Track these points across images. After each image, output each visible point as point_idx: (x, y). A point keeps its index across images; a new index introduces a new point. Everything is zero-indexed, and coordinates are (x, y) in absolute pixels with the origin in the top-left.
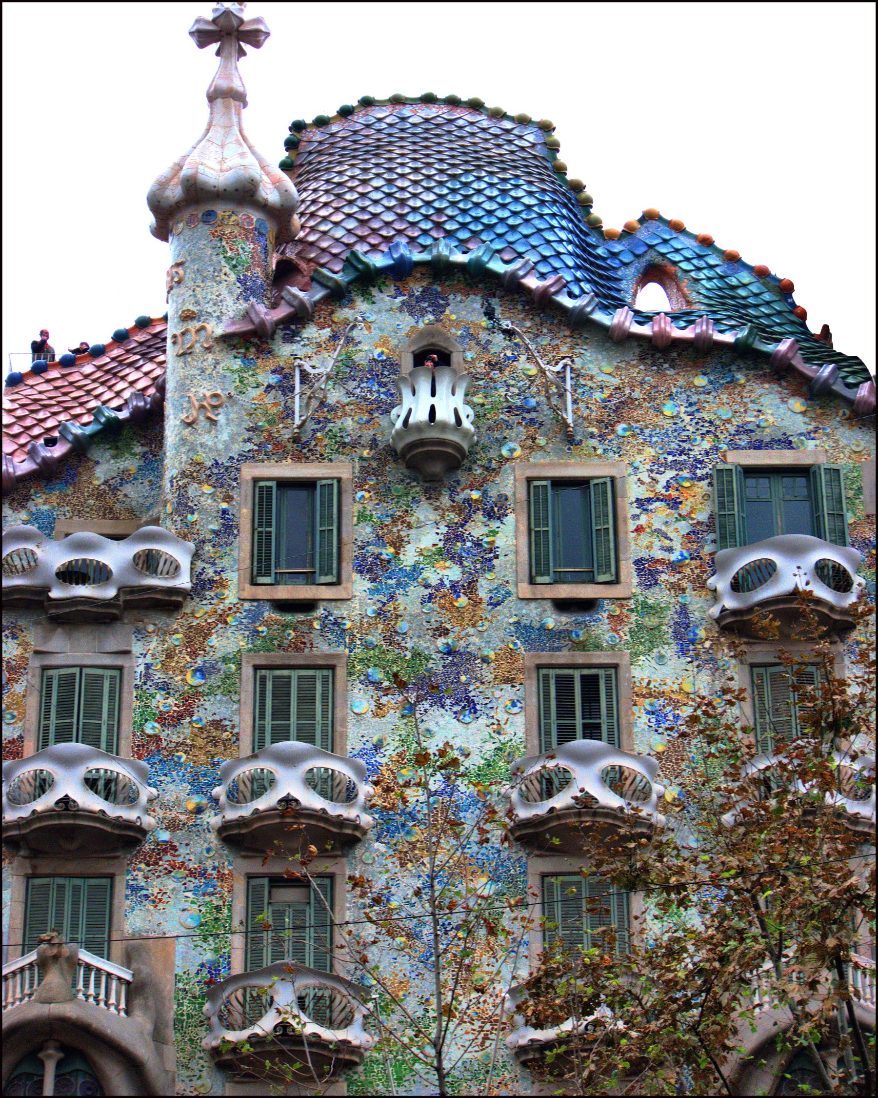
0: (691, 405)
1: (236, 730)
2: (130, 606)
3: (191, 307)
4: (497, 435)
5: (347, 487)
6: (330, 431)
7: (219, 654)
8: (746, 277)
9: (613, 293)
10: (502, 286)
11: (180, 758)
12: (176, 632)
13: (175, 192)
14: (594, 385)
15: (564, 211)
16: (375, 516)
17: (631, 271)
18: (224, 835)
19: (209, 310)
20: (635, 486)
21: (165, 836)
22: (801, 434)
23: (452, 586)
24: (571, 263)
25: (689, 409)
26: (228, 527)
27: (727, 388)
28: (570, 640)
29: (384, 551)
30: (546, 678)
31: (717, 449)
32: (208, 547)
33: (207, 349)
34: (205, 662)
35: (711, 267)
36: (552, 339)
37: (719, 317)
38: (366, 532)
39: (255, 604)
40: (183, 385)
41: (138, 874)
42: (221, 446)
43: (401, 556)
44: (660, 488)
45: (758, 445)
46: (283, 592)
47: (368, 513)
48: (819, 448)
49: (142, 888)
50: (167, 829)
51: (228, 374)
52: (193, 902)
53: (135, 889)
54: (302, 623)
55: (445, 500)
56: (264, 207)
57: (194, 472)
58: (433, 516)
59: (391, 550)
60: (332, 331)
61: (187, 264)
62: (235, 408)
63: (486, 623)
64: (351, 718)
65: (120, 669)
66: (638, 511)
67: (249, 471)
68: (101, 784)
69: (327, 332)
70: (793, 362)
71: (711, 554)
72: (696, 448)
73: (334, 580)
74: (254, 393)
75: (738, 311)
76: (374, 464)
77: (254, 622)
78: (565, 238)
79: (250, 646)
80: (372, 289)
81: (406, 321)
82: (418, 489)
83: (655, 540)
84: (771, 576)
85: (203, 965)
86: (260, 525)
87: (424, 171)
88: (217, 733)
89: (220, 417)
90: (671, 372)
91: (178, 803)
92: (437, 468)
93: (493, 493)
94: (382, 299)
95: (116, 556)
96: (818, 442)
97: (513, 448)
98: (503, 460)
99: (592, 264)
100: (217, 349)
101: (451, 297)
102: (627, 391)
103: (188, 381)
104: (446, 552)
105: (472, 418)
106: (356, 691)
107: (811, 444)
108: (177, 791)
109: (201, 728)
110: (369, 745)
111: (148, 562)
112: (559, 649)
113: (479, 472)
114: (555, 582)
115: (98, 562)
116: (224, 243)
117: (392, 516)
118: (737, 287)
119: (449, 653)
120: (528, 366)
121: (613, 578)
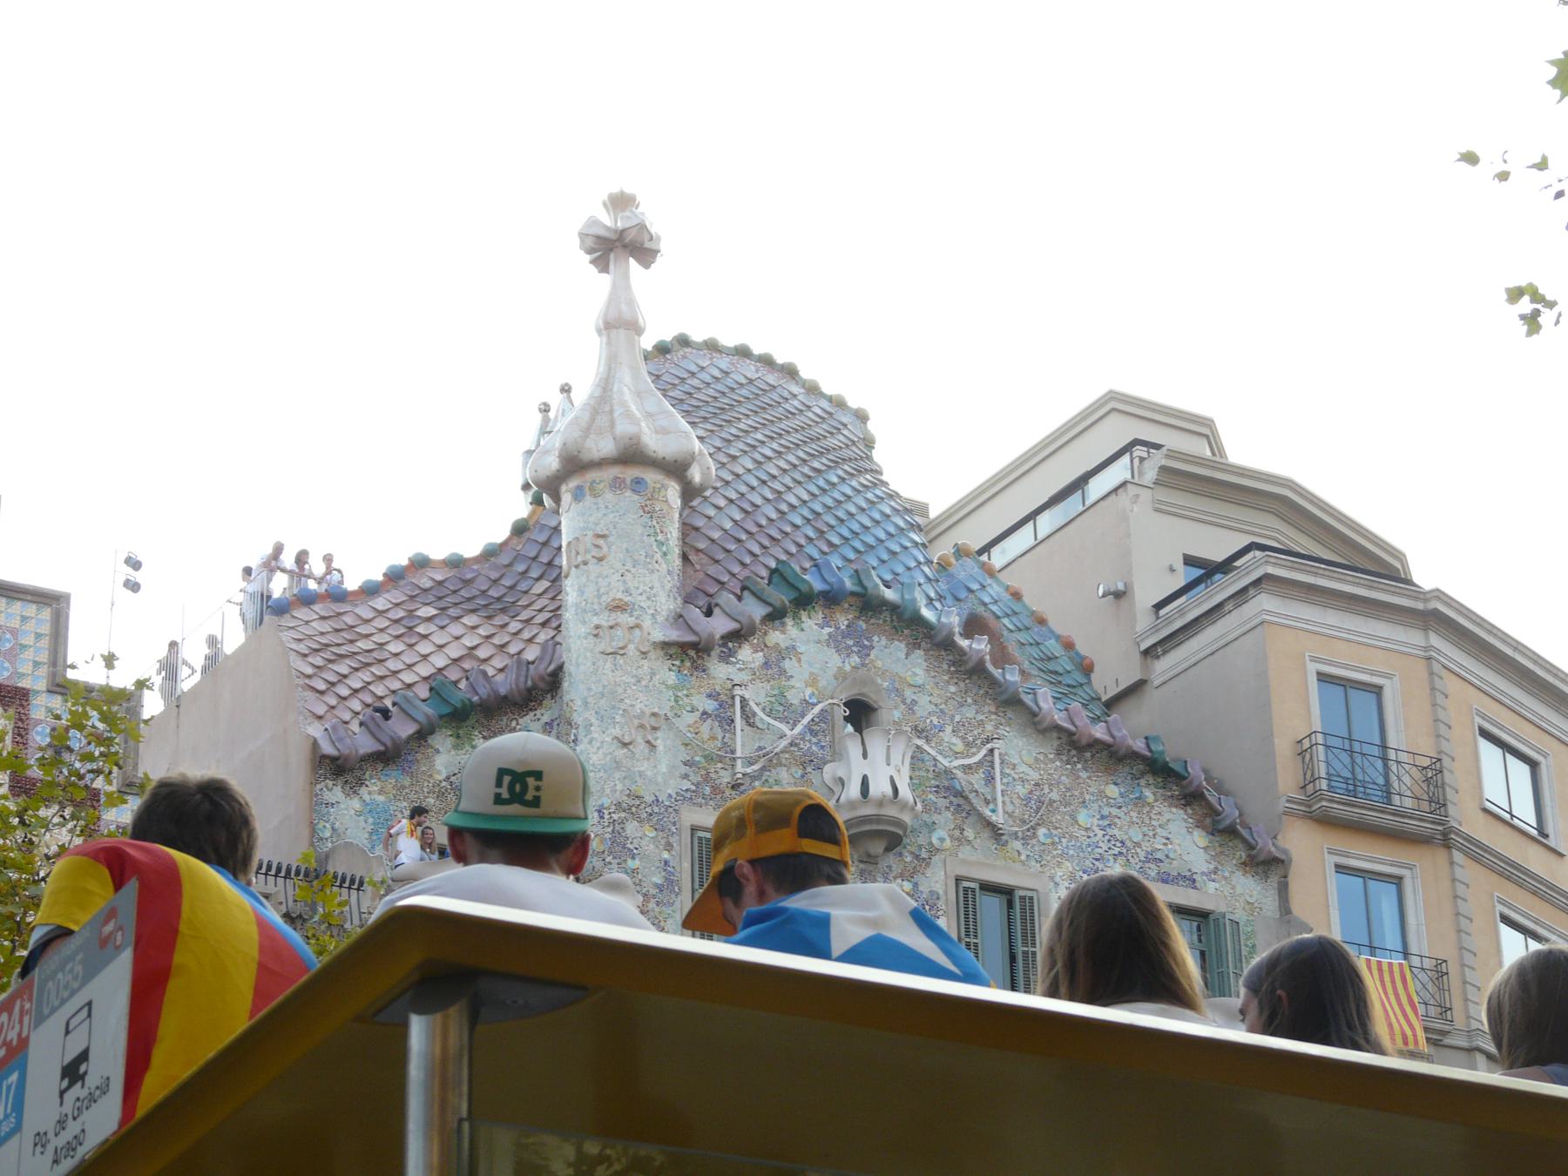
0: (1103, 817)
22: (1203, 873)
27: (1136, 805)
61: (611, 539)
90: (1084, 775)
92: (877, 847)
100: (652, 655)
101: (876, 638)
107: (1212, 885)
120: (954, 740)
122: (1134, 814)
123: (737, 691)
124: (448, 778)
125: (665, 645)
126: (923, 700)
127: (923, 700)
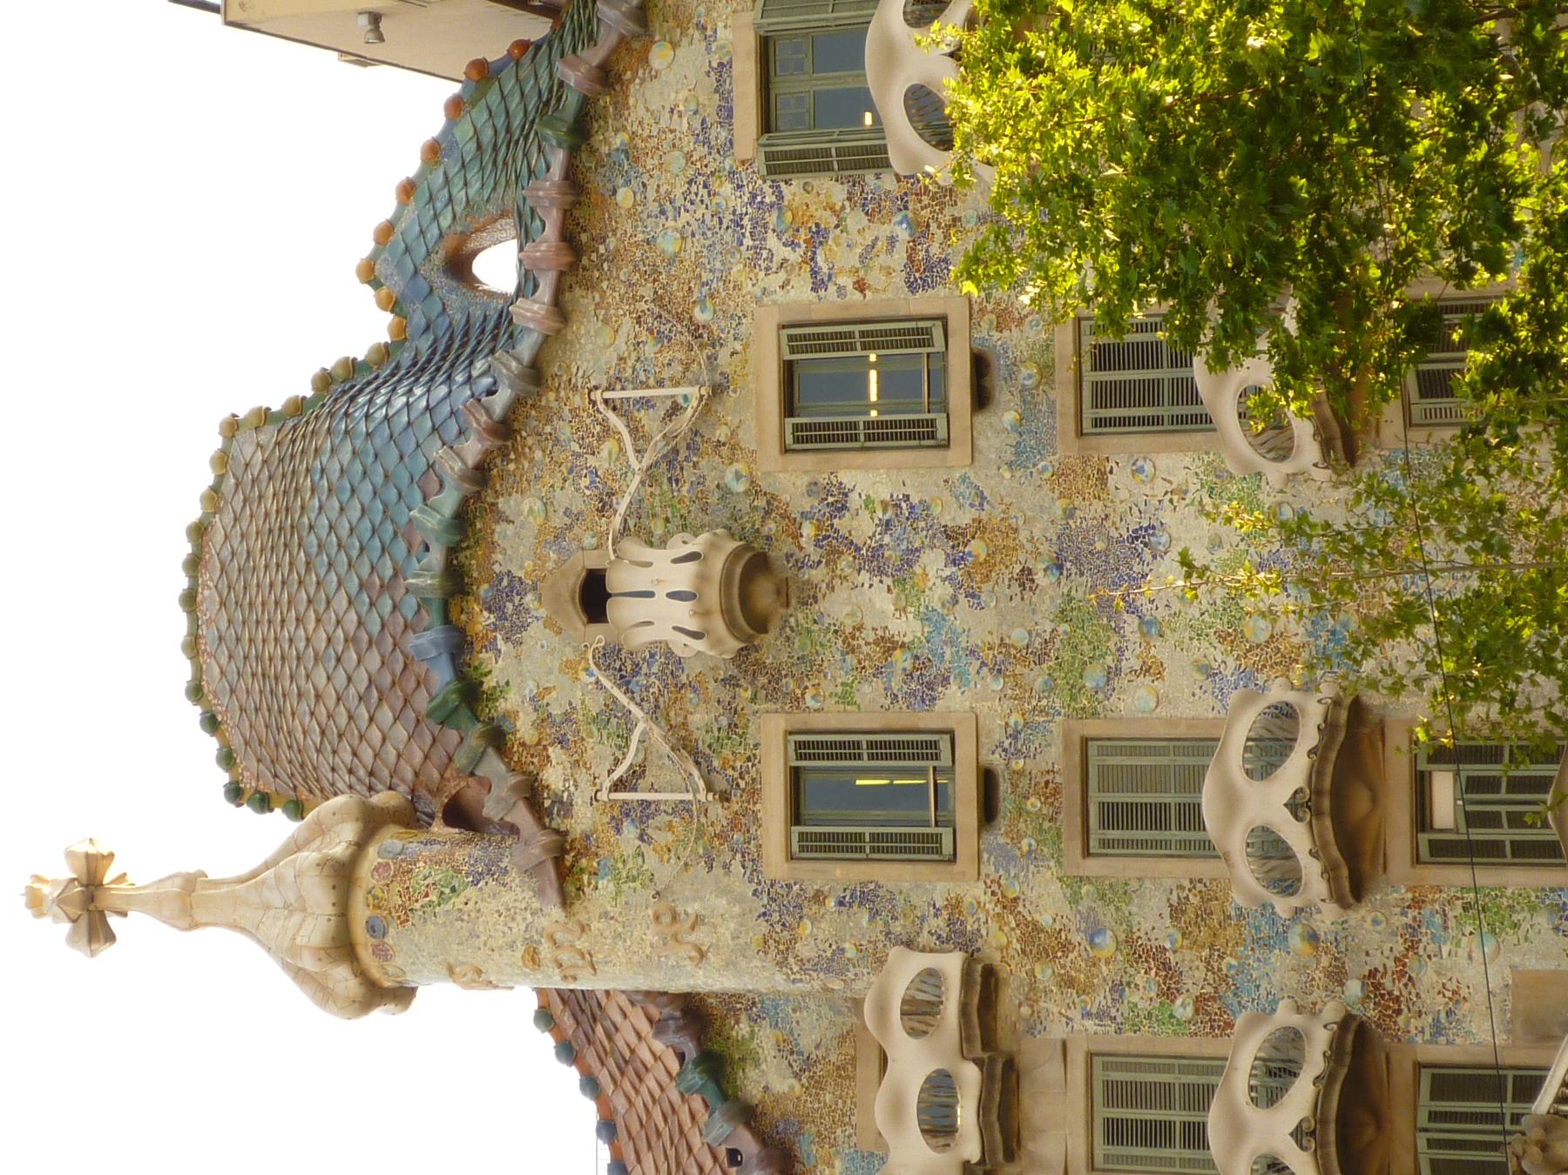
0: (663, 212)
1: (1187, 884)
2: (988, 1042)
3: (519, 954)
4: (713, 499)
5: (799, 720)
6: (710, 746)
7: (1066, 909)
8: (464, 131)
9: (489, 327)
10: (479, 493)
11: (1230, 967)
12: (1031, 973)
13: (342, 977)
14: (634, 356)
15: (361, 400)
16: (844, 679)
17: (454, 300)
18: (1351, 900)
19: (523, 927)
20: (792, 293)
21: (1354, 988)
22: (708, 49)
23: (954, 563)
24: (444, 390)
25: (670, 214)
26: (864, 897)
28: (1037, 387)
29: (900, 665)
30: (1098, 422)
31: (732, 173)
32: (897, 928)
33: (583, 930)
34: (1078, 930)
35: (447, 181)
36: (561, 418)
37: (525, 170)
38: (870, 692)
39: (985, 856)
40: (639, 964)
41: (1413, 1026)
42: (737, 909)
43: (906, 640)
44: (794, 256)
45: (727, 114)
46: (966, 811)
47: (839, 689)
48: (729, 22)
49: (1437, 1021)
50: (1342, 984)
51: (622, 899)
52: (1458, 945)
53: (1437, 1029)
54: (1014, 785)
55: (818, 575)
56: (361, 845)
57: (780, 948)
58: (842, 592)
59: (898, 653)
60: (552, 744)
61: (452, 961)
62: (676, 887)
63: (1012, 513)
64: (1163, 712)
65: (1091, 1056)
66: (832, 289)
67: (775, 863)
68: (1273, 1083)
69: (554, 752)
70: (595, 62)
71: (899, 180)
72: (731, 204)
73: (947, 737)
74: (652, 861)
75: (517, 142)
76: (763, 680)
77: (1014, 857)
78: (404, 399)
79: (1052, 863)
80: (485, 687)
81: (536, 633)
82: (800, 616)
83: (876, 263)
84: (930, 93)
85: (1556, 929)
86: (862, 850)
87: (302, 609)
88: (1198, 913)
89: (689, 910)
90: (612, 242)
91: (1301, 968)
93: (807, 504)
94: (501, 670)
95: (913, 1062)
96: (720, 25)
97: (733, 477)
98: (755, 490)
99: (444, 359)
102: (642, 306)
103: (629, 959)
104: (901, 574)
105: (686, 536)
106: (1122, 705)
107: (722, 34)
108: (1279, 970)
109: (1184, 935)
110: (1208, 684)
111: (920, 1013)
112: (1052, 405)
113: (773, 526)
114: (944, 408)
115: (922, 1090)
116: (417, 906)
117: (844, 654)
118: (479, 147)
119: (1060, 567)
120: (604, 454)
121: (939, 323)
122: (650, 163)
123: (603, 796)
124: (797, 1076)
125: (566, 902)
126: (563, 498)
127: (563, 498)
